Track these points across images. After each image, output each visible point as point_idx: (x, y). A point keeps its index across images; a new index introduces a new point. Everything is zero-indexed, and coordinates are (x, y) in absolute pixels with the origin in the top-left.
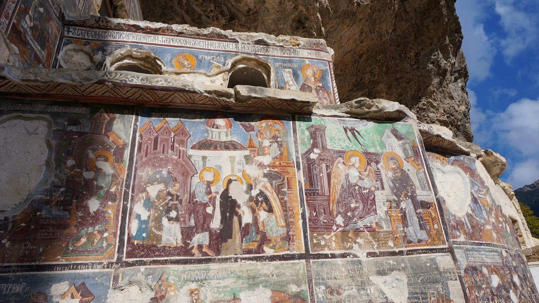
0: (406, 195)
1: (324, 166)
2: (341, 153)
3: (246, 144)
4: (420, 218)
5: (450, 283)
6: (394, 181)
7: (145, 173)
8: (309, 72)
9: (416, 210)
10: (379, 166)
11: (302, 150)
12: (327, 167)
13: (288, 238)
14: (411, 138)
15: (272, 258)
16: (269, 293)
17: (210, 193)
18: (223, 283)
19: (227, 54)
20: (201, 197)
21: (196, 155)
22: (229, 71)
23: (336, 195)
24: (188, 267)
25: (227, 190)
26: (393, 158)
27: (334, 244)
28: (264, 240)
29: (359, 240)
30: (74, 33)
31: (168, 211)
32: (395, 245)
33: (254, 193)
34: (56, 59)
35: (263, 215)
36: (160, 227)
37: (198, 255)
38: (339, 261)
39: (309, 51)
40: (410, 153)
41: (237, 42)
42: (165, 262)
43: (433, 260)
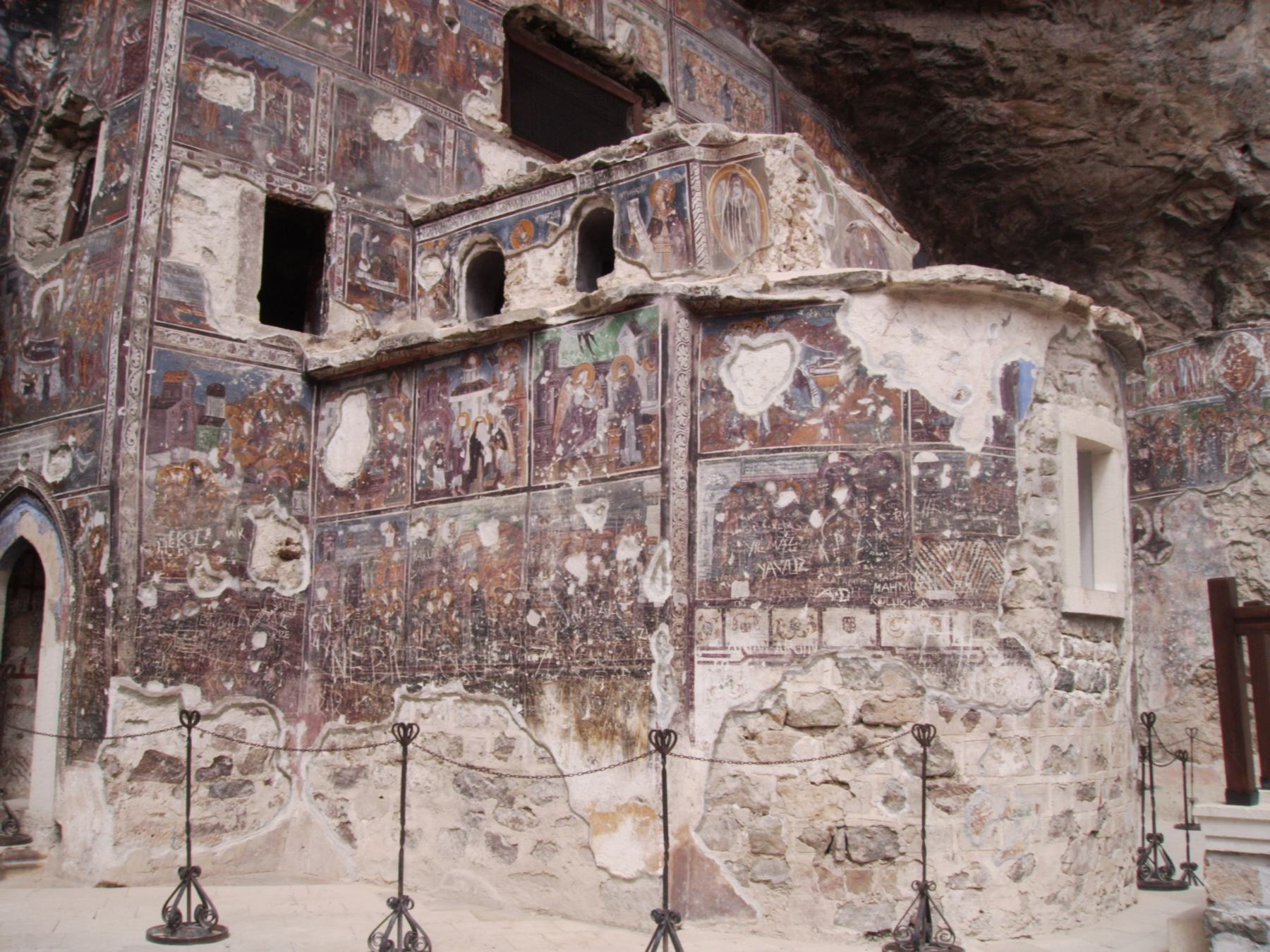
0: (630, 410)
1: (552, 390)
2: (570, 371)
3: (489, 382)
4: (639, 436)
5: (650, 508)
6: (619, 394)
7: (423, 427)
8: (659, 196)
9: (636, 425)
10: (607, 378)
11: (535, 375)
12: (556, 390)
13: (516, 474)
14: (653, 328)
15: (504, 493)
16: (497, 524)
17: (462, 438)
18: (469, 517)
19: (562, 205)
20: (458, 444)
21: (453, 400)
22: (571, 227)
23: (560, 423)
24: (450, 505)
25: (474, 435)
26: (625, 363)
27: (551, 475)
28: (499, 477)
29: (575, 469)
30: (425, 234)
31: (436, 459)
32: (609, 471)
33: (494, 431)
34: (414, 278)
35: (500, 452)
36: (432, 475)
37: (455, 496)
38: (554, 491)
39: (659, 155)
40: (646, 351)
41: (572, 177)
42: (436, 503)
43: (640, 485)
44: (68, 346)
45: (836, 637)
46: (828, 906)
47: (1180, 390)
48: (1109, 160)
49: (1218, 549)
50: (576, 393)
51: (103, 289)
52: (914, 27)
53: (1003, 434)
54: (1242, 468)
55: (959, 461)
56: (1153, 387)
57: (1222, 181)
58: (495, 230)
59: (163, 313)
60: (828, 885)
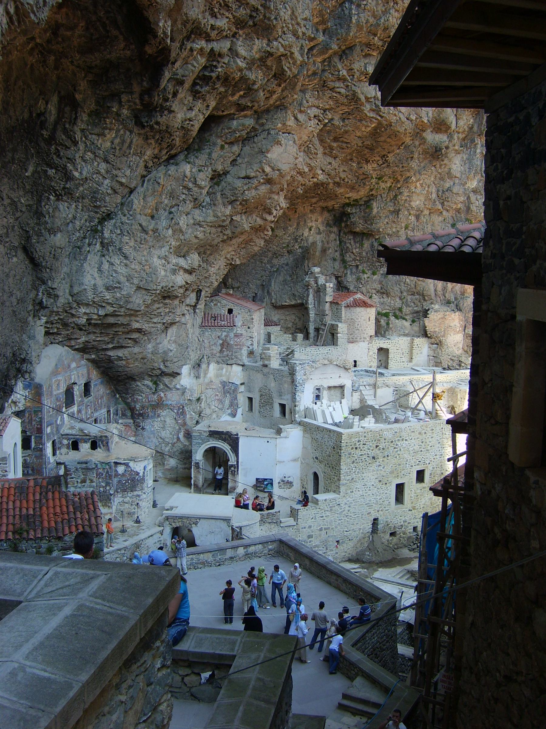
19: (89, 439)
30: (64, 437)
44: (33, 467)
45: (129, 495)
46: (129, 519)
47: (149, 401)
48: (141, 368)
49: (154, 430)
50: (101, 471)
51: (39, 462)
52: (111, 353)
53: (144, 473)
54: (159, 416)
55: (140, 477)
56: (144, 400)
57: (160, 369)
58: (78, 439)
59: (48, 465)
60: (129, 517)
